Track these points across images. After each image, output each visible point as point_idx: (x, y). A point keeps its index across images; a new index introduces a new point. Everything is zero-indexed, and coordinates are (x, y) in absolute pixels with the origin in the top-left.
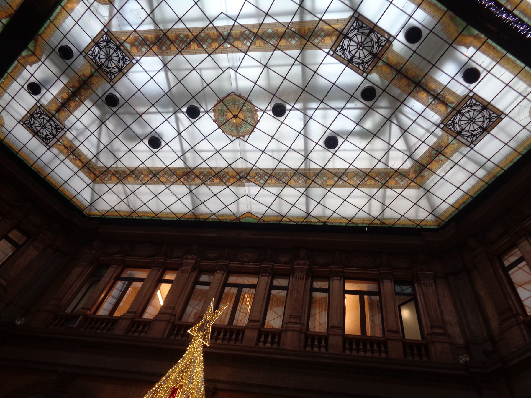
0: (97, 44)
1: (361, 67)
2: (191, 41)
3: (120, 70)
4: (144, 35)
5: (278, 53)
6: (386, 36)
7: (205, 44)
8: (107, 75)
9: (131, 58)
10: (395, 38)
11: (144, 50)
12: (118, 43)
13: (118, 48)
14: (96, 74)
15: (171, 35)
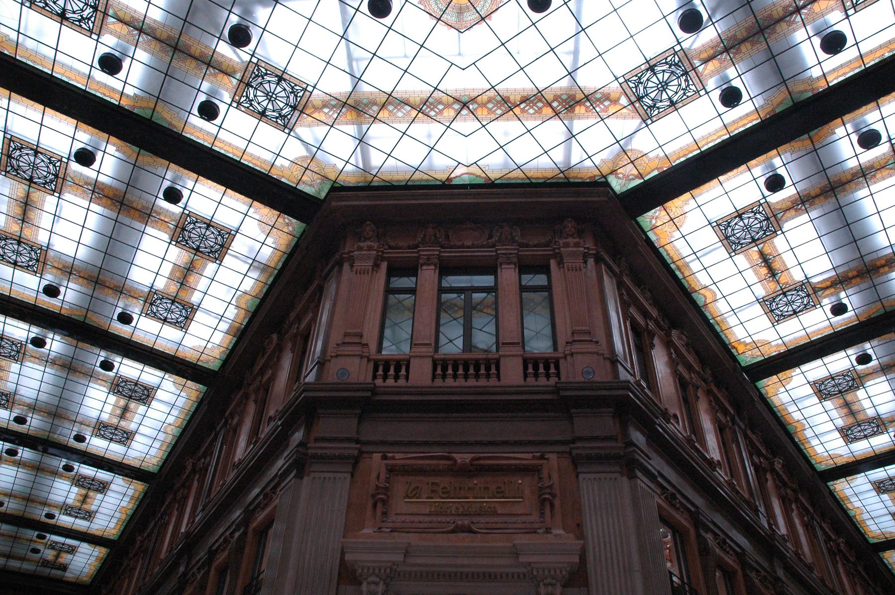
0: (673, 104)
1: (263, 70)
2: (518, 105)
3: (651, 68)
4: (590, 114)
5: (389, 91)
6: (243, 109)
7: (498, 102)
8: (680, 61)
9: (625, 85)
10: (230, 105)
11: (598, 96)
12: (637, 105)
13: (640, 99)
14: (697, 63)
15: (548, 111)
